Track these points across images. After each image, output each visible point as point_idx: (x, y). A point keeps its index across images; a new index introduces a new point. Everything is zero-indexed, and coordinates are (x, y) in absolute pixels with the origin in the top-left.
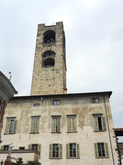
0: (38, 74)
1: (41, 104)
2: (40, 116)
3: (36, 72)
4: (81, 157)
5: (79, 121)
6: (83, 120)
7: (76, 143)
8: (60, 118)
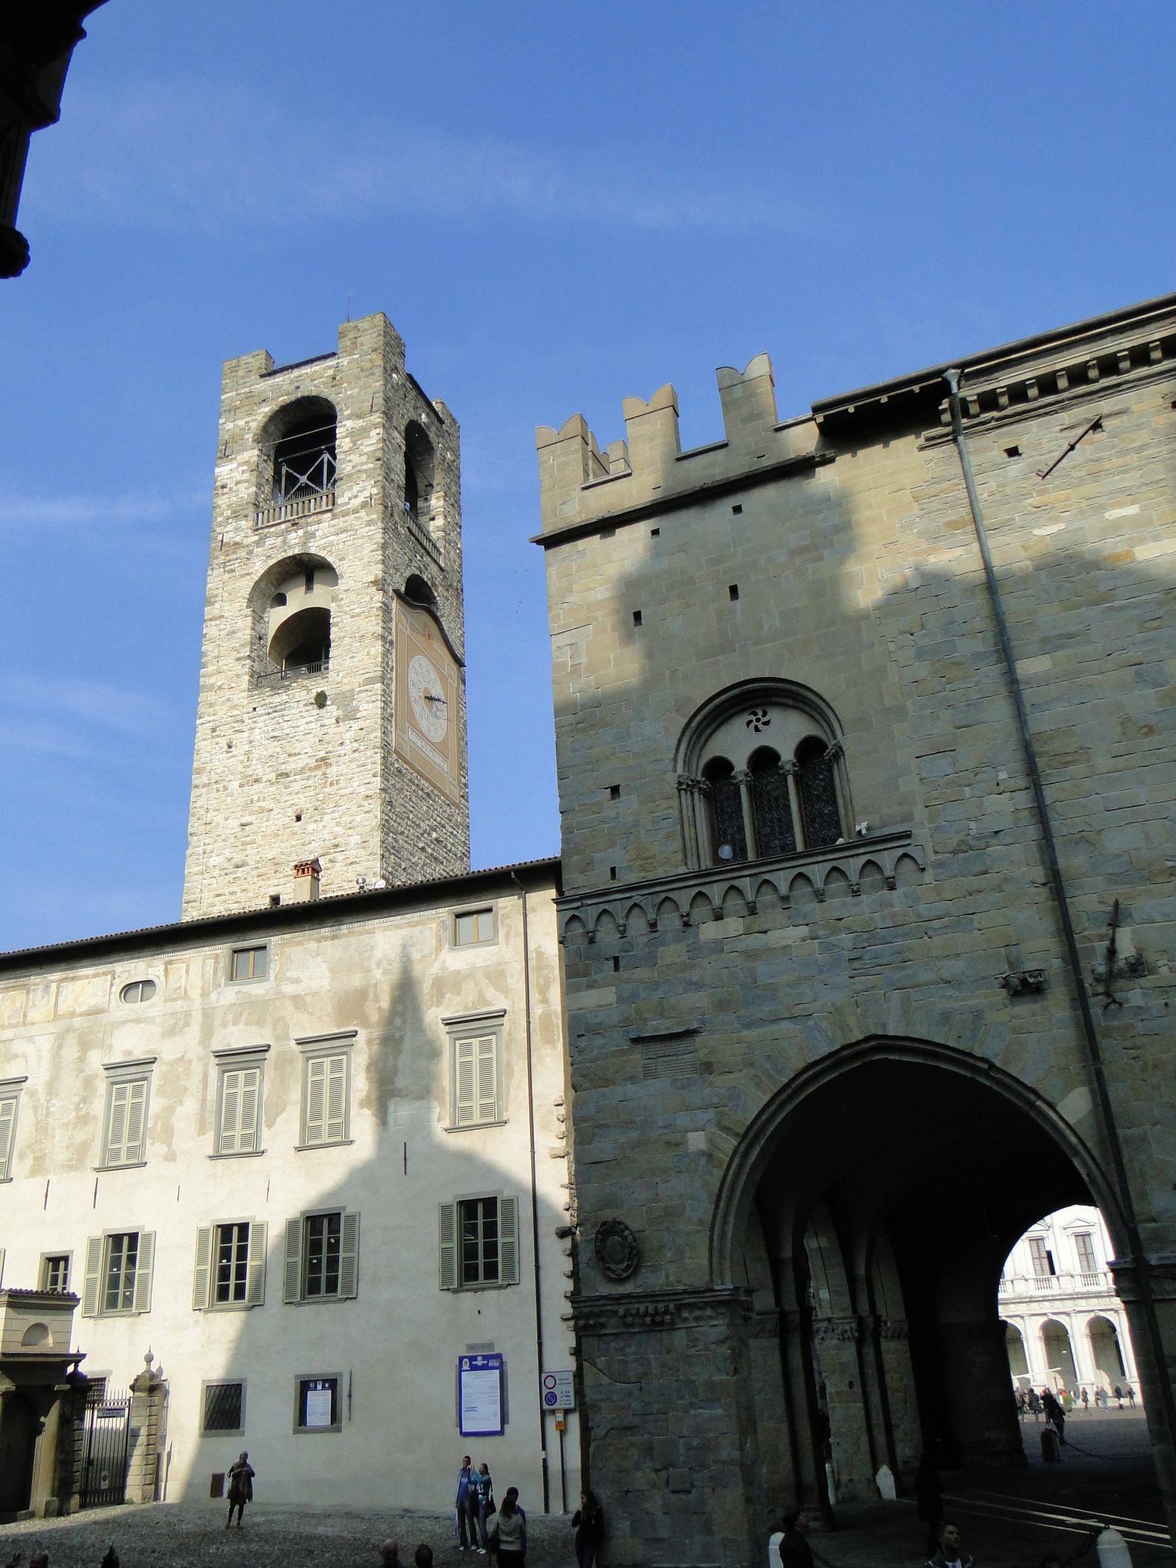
2: (153, 1061)
3: (214, 730)
4: (364, 1290)
6: (390, 1064)
7: (344, 1208)
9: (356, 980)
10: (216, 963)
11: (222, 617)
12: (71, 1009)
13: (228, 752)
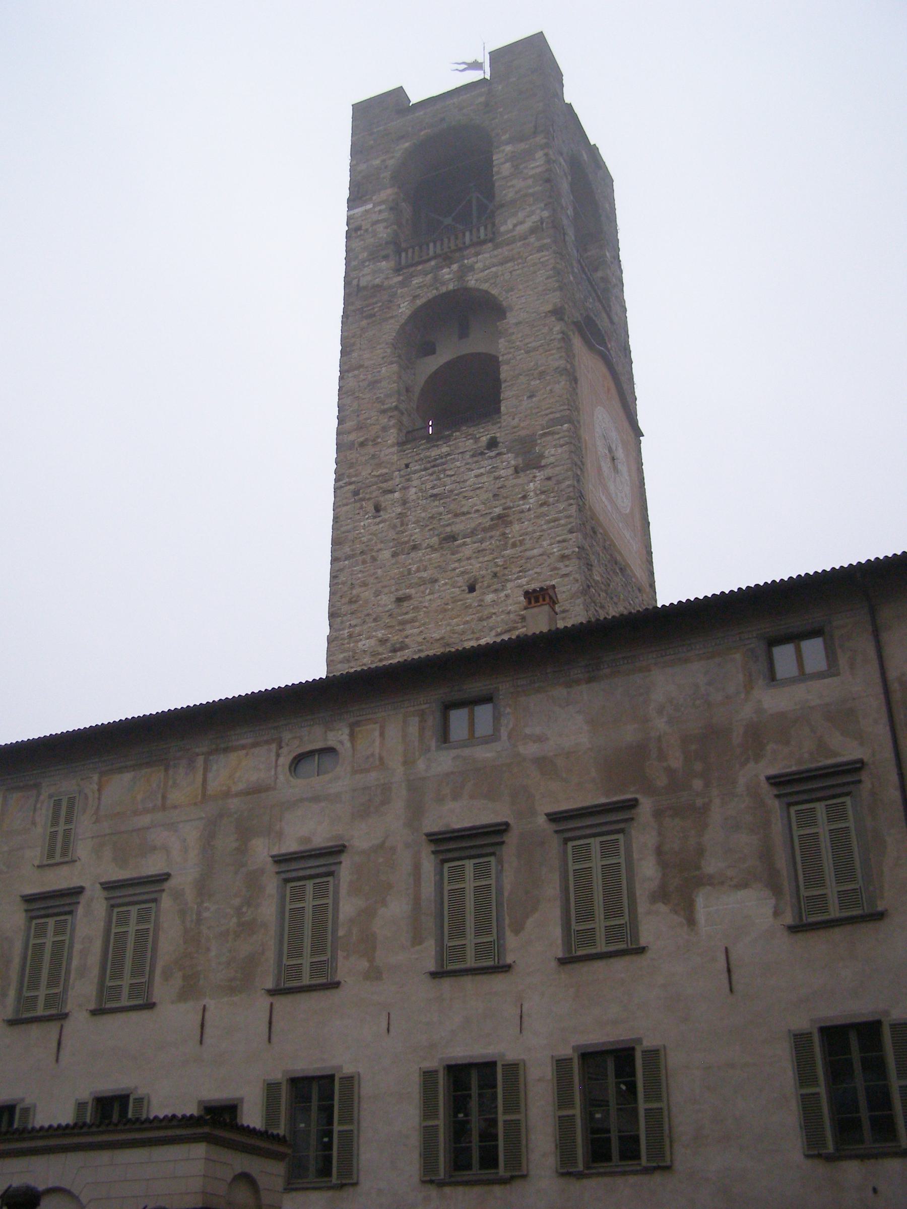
0: (377, 509)
1: (348, 744)
5: (659, 851)
7: (639, 1041)
8: (503, 843)
9: (629, 734)
10: (423, 721)
11: (361, 366)
12: (224, 788)
13: (375, 517)
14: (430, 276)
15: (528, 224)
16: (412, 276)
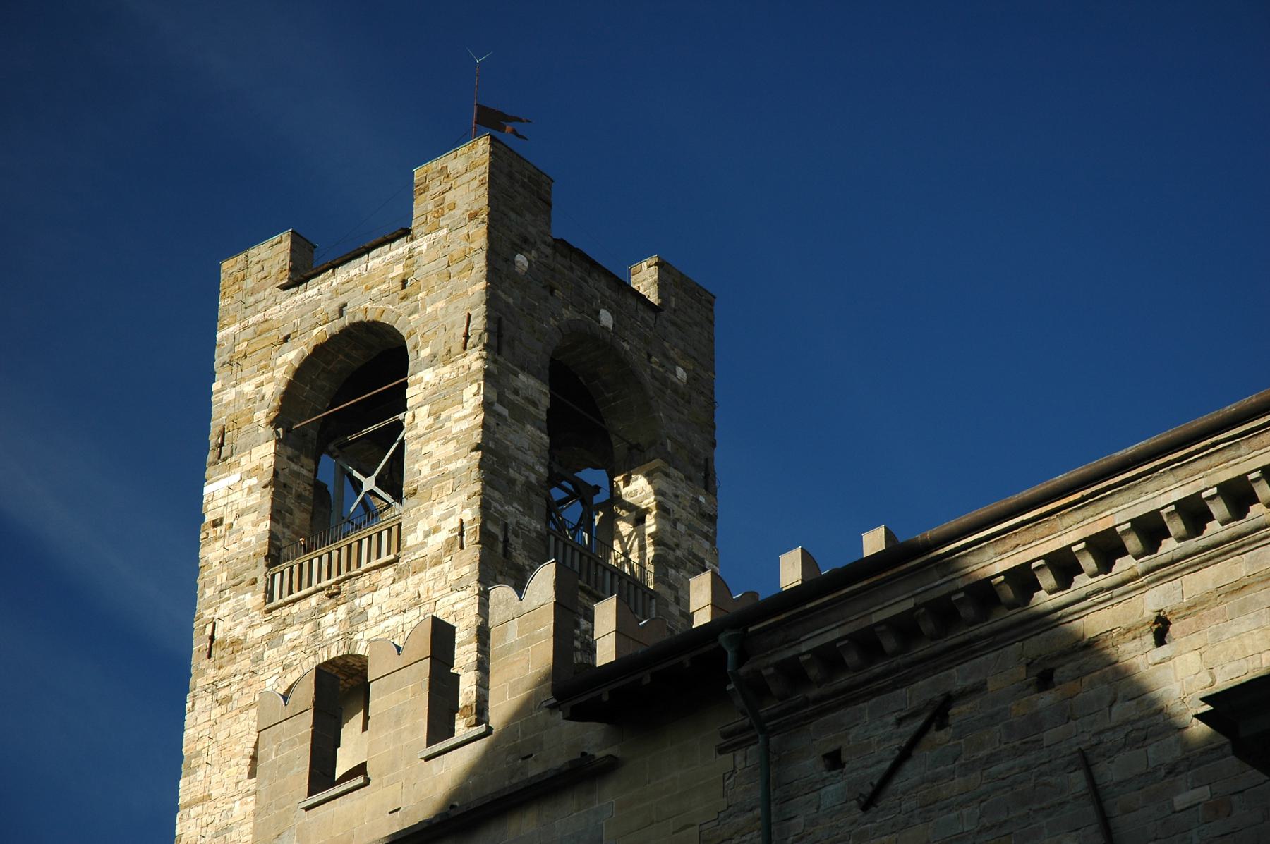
14: (308, 626)
15: (442, 536)
16: (286, 624)
